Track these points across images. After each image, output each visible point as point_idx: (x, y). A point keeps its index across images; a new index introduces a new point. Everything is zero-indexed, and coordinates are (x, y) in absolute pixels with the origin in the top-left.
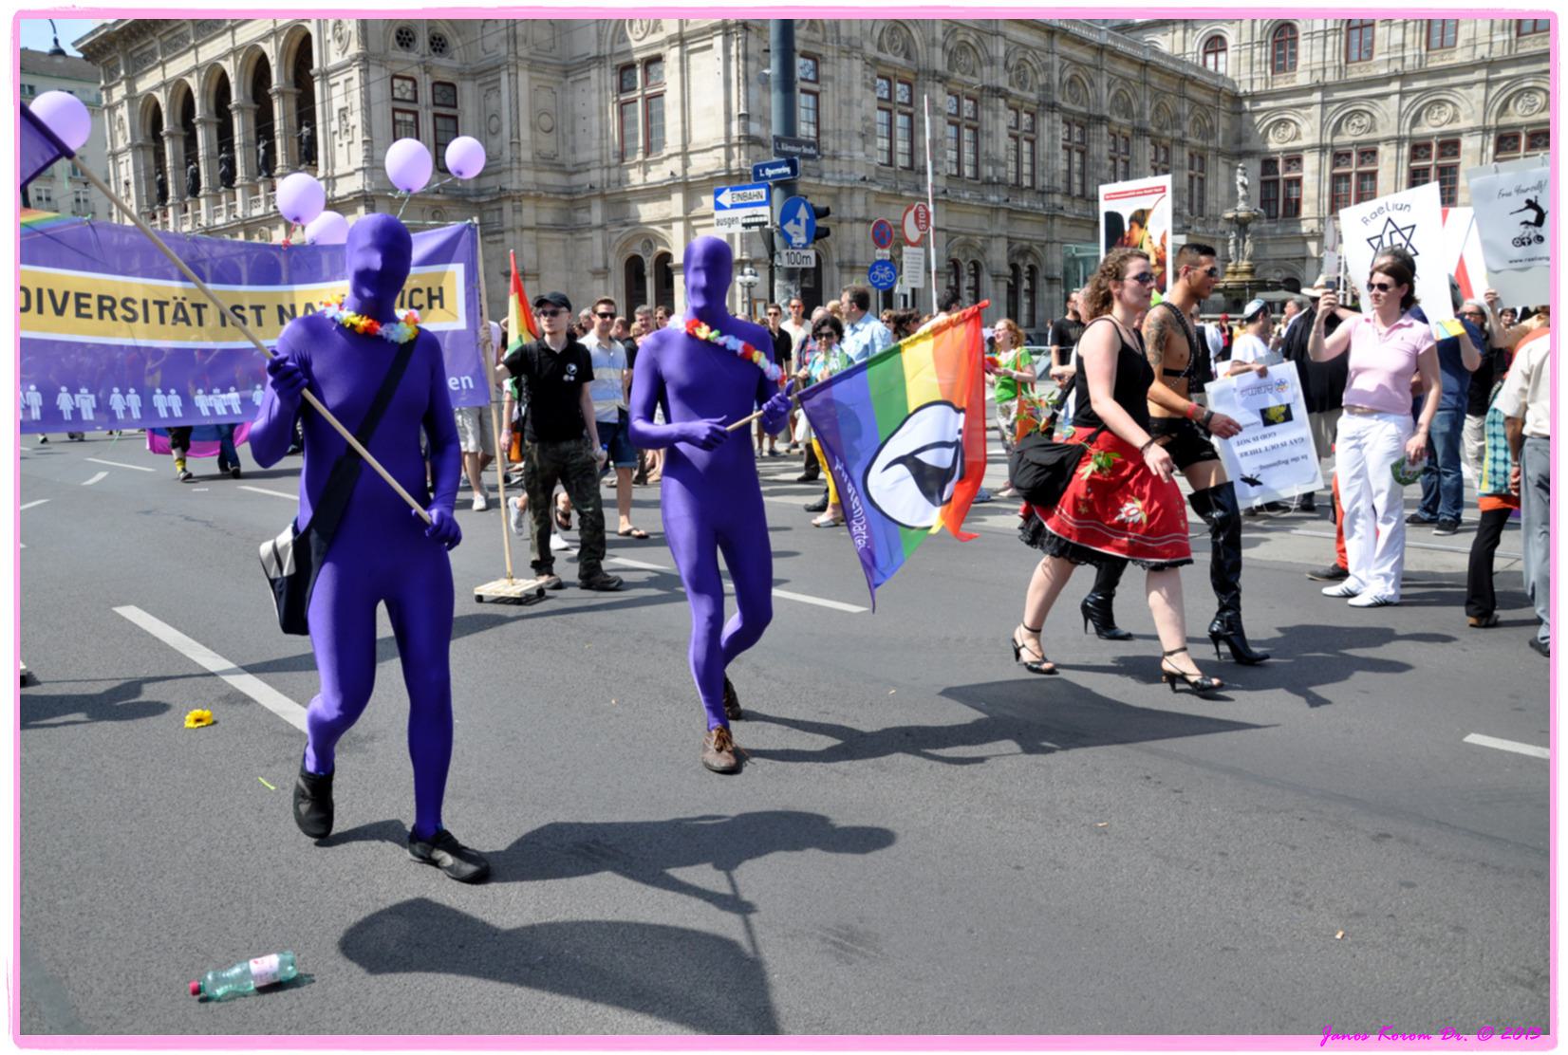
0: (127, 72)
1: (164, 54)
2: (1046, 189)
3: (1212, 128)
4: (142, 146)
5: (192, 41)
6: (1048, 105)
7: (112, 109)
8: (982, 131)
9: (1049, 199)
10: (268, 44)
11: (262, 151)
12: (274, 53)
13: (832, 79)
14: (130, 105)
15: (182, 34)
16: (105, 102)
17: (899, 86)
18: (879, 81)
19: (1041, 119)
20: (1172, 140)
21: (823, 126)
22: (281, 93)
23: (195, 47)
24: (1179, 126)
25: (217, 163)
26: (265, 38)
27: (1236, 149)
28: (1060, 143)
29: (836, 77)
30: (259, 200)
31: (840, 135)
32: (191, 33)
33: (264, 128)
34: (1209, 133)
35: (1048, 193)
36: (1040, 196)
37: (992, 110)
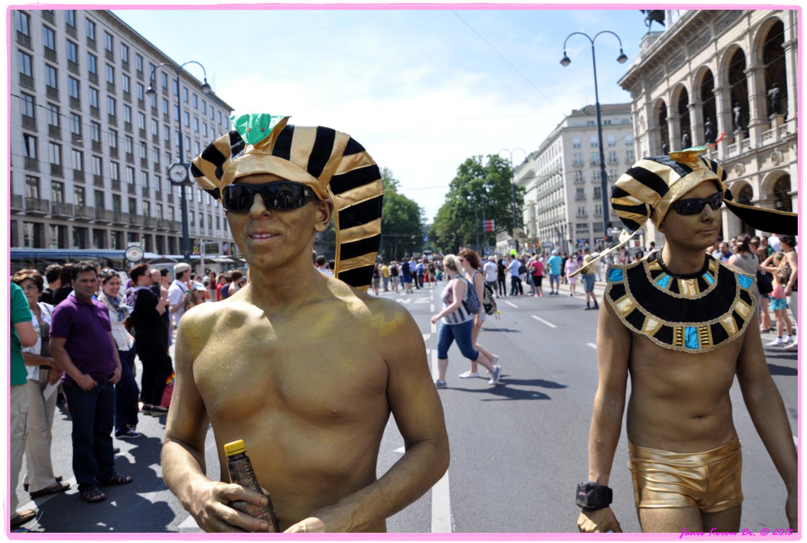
0: (646, 90)
1: (668, 72)
4: (654, 130)
5: (687, 58)
7: (637, 113)
10: (744, 41)
11: (737, 114)
12: (748, 45)
14: (648, 108)
15: (680, 57)
16: (633, 110)
22: (753, 70)
23: (689, 61)
25: (702, 129)
26: (741, 38)
30: (735, 147)
32: (686, 53)
33: (739, 97)
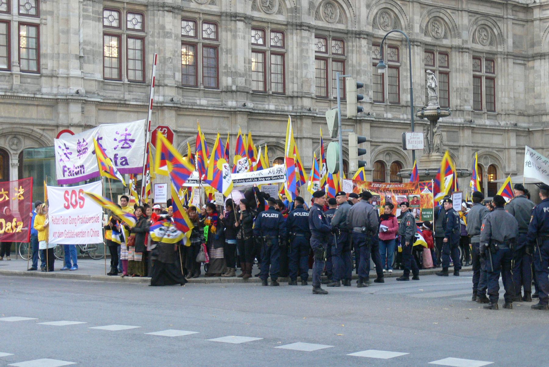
2: (295, 94)
3: (501, 35)
6: (297, 25)
8: (222, 49)
9: (299, 102)
13: (51, 13)
17: (130, 17)
18: (106, 13)
19: (290, 36)
20: (451, 48)
21: (43, 50)
24: (459, 35)
27: (530, 52)
28: (312, 55)
29: (55, 12)
31: (59, 57)
34: (501, 38)
35: (297, 97)
36: (290, 99)
37: (231, 31)
